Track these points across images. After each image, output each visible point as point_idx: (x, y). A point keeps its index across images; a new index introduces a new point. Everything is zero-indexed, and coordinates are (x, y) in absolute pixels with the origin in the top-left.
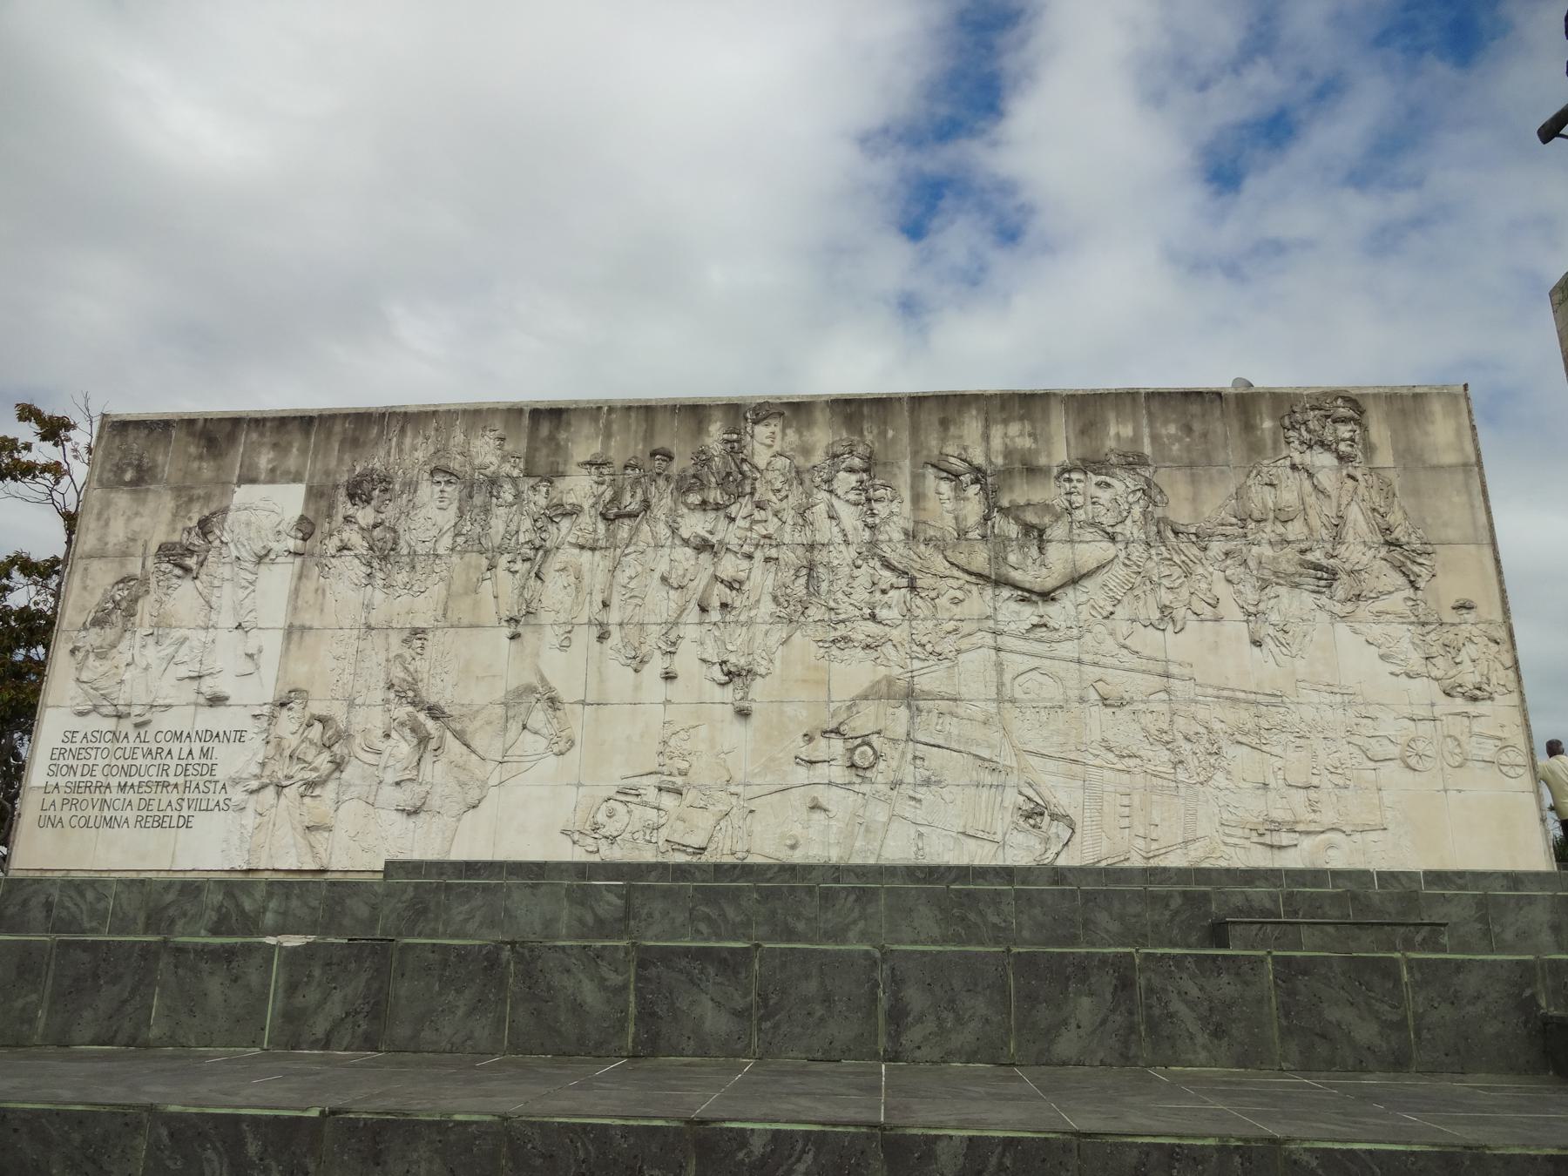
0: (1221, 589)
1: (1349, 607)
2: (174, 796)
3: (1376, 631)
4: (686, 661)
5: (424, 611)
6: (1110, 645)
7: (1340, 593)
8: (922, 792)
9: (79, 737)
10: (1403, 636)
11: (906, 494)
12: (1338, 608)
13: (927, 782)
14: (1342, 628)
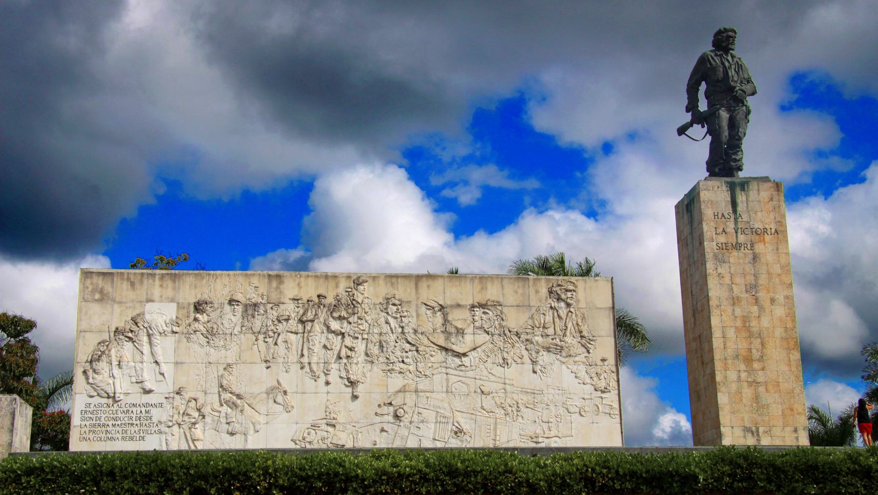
0: (525, 353)
1: (567, 359)
2: (137, 429)
3: (574, 368)
4: (333, 377)
5: (230, 356)
6: (485, 372)
7: (564, 354)
8: (421, 425)
9: (92, 406)
10: (582, 368)
11: (414, 314)
12: (563, 360)
13: (423, 421)
14: (564, 367)
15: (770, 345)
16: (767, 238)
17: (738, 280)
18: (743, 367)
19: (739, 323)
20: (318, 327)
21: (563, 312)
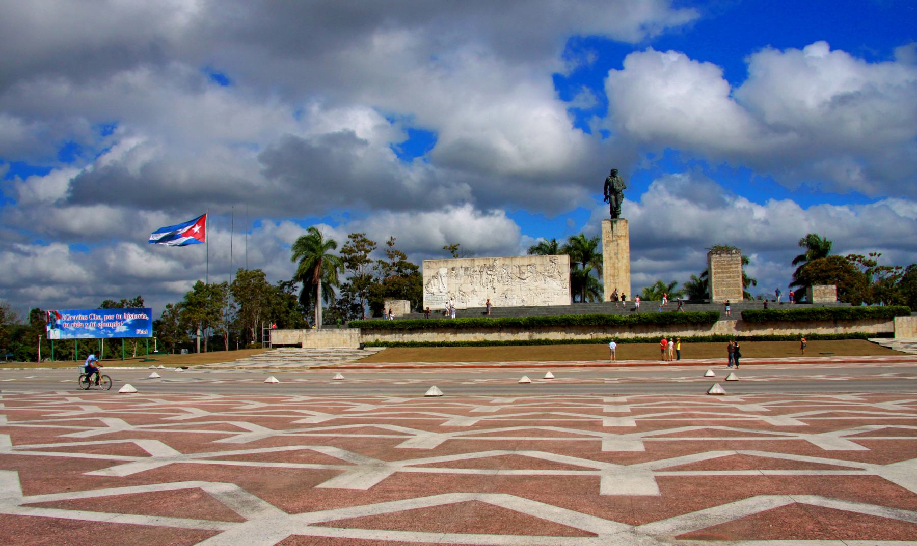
5: (462, 282)
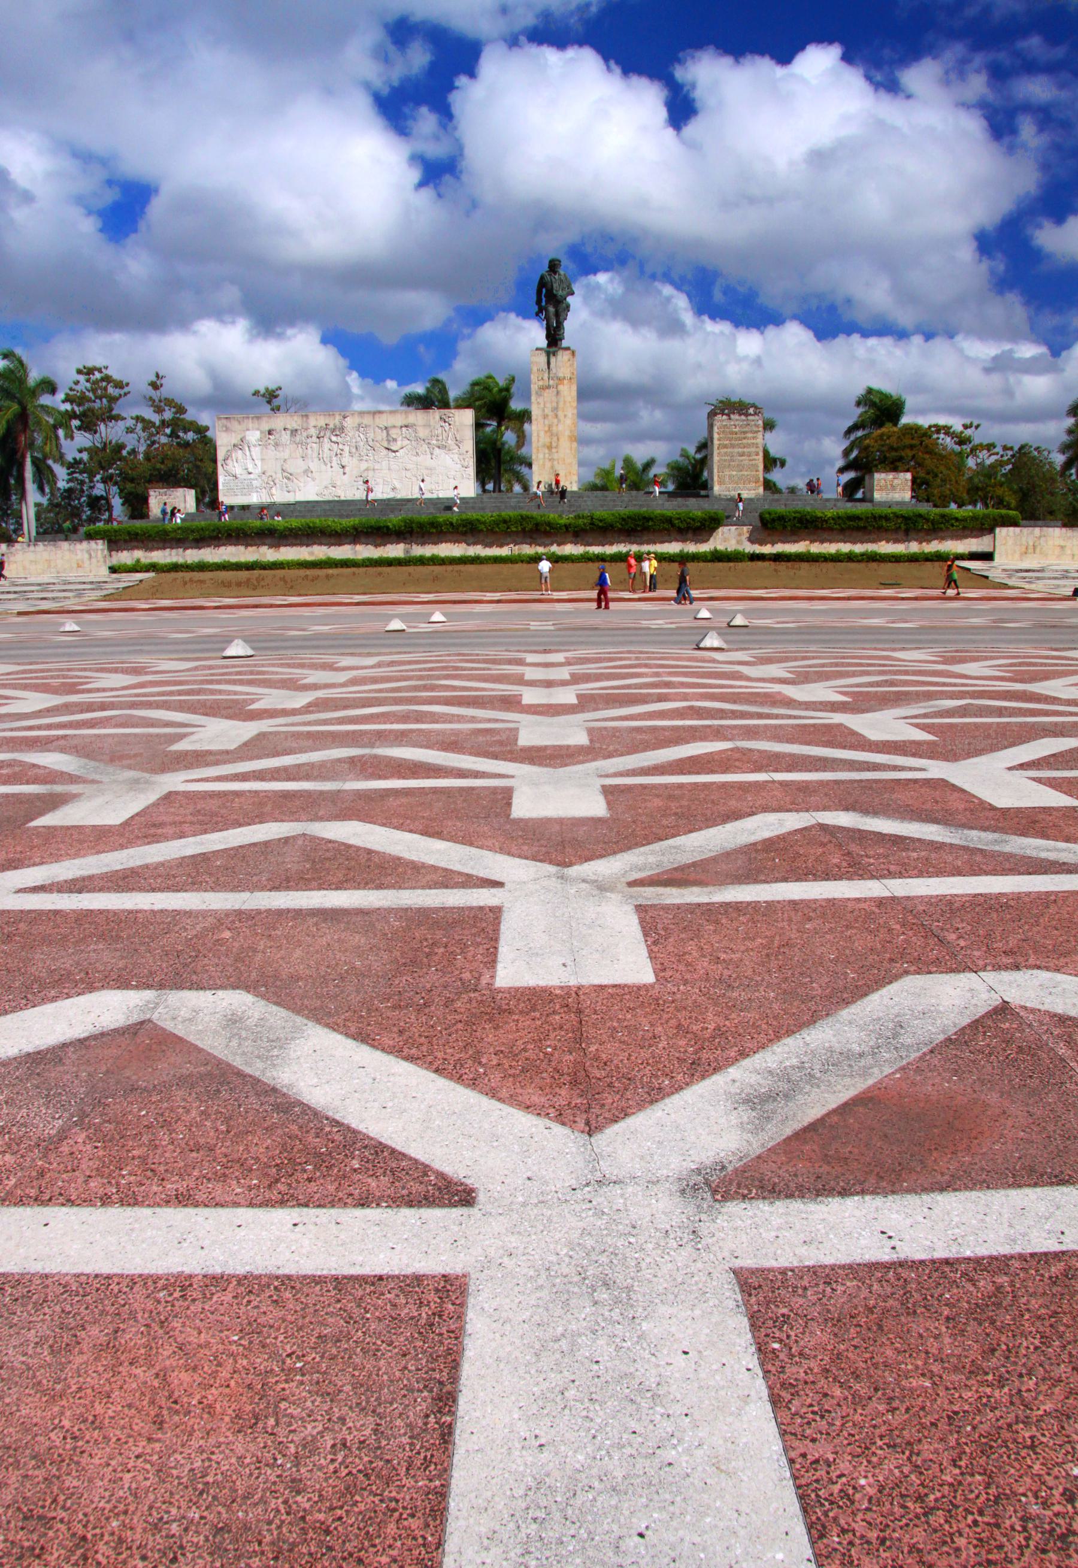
4: (334, 464)
10: (456, 456)
15: (562, 440)
16: (566, 382)
17: (548, 405)
18: (547, 451)
19: (546, 429)
20: (326, 440)
21: (447, 428)
